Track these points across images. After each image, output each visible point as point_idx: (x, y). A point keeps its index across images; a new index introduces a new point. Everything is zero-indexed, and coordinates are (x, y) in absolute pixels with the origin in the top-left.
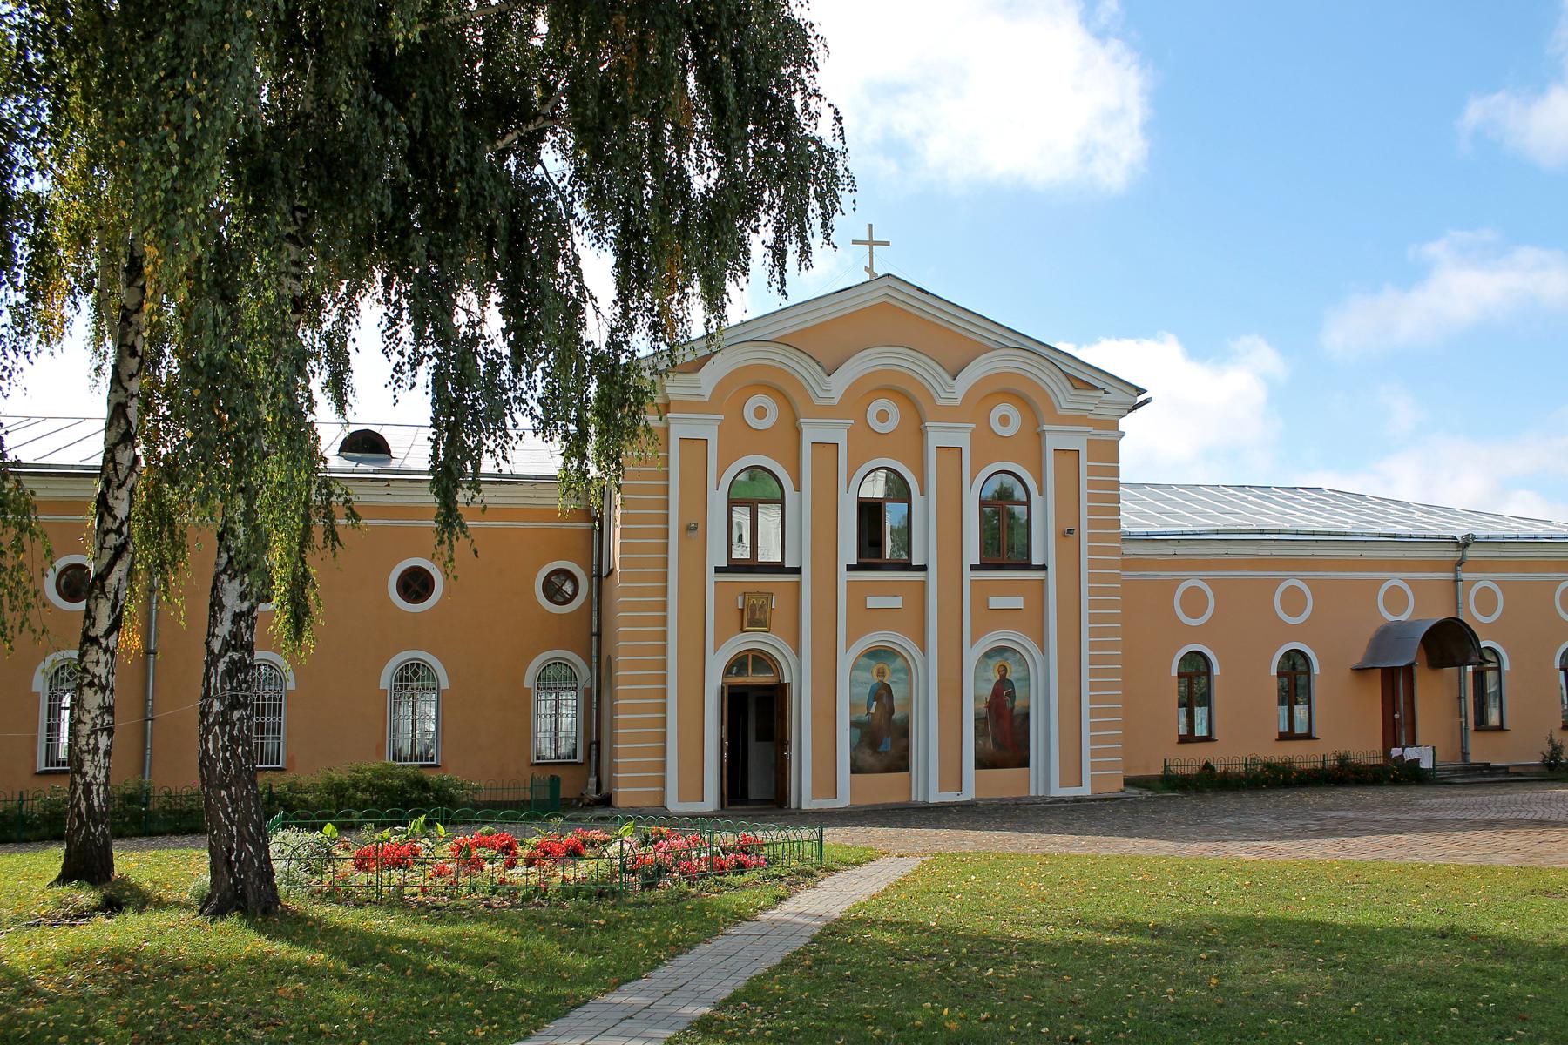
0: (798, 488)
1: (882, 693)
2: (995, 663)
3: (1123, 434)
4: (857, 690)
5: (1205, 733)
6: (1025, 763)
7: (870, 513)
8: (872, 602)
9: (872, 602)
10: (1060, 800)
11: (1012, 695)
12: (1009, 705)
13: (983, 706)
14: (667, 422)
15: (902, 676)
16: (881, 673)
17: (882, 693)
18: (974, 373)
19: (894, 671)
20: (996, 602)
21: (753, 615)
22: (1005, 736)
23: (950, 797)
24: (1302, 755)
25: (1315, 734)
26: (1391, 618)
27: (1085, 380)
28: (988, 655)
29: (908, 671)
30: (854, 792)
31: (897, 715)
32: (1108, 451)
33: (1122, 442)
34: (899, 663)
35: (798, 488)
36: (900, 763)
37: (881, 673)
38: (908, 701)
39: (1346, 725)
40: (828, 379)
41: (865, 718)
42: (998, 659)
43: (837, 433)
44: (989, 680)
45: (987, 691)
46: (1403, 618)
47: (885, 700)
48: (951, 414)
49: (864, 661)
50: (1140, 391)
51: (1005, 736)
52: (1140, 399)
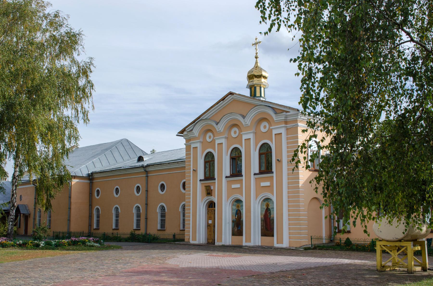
2: (265, 203)
4: (233, 211)
12: (269, 217)
13: (263, 216)
16: (238, 207)
20: (263, 184)
22: (268, 228)
23: (248, 244)
37: (238, 207)
42: (266, 202)
44: (264, 208)
45: (264, 213)
47: (239, 215)
49: (235, 203)
51: (268, 228)
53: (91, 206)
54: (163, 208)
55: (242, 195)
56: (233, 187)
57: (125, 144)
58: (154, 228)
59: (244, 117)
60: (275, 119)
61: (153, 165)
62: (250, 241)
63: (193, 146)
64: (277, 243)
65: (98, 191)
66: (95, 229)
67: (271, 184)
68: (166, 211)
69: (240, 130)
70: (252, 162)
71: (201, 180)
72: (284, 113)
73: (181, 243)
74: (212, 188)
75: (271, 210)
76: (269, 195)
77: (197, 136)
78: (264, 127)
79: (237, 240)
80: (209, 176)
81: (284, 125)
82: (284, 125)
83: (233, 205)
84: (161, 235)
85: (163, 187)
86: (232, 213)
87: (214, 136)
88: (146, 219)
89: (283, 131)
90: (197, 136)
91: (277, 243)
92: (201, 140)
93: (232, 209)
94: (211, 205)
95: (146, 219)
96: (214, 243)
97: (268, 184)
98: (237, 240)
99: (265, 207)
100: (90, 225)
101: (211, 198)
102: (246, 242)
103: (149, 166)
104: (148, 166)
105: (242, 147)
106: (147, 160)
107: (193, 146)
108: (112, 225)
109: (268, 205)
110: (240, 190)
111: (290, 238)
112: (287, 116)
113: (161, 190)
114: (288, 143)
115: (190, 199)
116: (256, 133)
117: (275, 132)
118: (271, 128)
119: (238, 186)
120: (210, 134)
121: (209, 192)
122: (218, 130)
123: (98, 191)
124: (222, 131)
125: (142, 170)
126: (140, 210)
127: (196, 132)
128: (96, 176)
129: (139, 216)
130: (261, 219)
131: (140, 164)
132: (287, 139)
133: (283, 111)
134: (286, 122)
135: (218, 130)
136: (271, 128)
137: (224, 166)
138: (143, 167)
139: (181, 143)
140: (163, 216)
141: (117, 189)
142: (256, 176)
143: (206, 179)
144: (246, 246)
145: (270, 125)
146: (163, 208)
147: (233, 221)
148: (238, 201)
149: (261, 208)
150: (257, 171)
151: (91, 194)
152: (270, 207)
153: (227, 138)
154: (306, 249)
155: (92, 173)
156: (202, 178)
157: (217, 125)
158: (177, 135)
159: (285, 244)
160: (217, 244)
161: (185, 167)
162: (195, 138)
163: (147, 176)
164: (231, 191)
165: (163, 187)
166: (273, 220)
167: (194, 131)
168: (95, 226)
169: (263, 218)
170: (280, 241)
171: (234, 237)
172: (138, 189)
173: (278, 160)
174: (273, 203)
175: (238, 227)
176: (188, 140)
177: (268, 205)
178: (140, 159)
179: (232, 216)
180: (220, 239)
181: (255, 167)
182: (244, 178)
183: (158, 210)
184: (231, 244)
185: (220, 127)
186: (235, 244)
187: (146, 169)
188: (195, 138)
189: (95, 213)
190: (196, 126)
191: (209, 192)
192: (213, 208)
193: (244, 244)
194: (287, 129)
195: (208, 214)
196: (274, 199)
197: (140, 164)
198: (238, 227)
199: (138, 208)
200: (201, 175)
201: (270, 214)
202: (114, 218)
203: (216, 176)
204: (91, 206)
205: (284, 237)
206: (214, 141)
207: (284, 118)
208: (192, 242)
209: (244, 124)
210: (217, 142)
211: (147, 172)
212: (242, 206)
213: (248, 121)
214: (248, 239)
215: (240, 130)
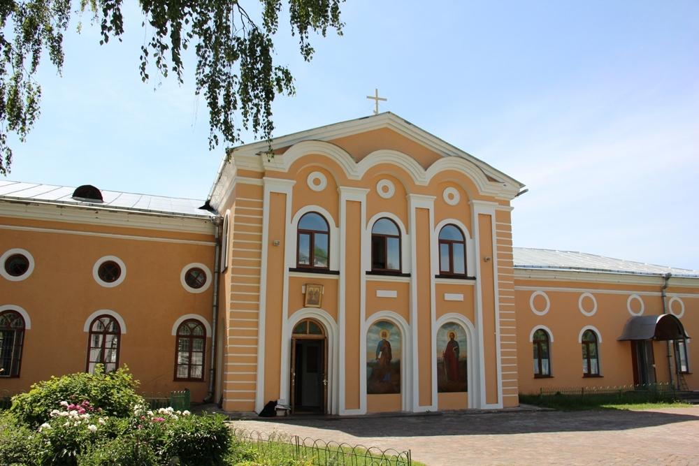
0: (338, 225)
1: (385, 348)
3: (512, 208)
4: (370, 345)
5: (547, 373)
6: (466, 390)
7: (379, 244)
8: (380, 293)
9: (380, 293)
10: (489, 412)
11: (457, 350)
12: (456, 355)
13: (441, 356)
14: (263, 183)
15: (396, 337)
16: (384, 335)
17: (385, 348)
18: (436, 168)
19: (392, 334)
21: (309, 299)
23: (424, 409)
24: (593, 386)
25: (690, 372)
26: (634, 315)
27: (493, 177)
29: (399, 334)
30: (369, 406)
31: (393, 360)
32: (505, 217)
33: (512, 212)
34: (394, 330)
35: (338, 225)
36: (395, 388)
38: (400, 351)
39: (615, 369)
40: (357, 165)
42: (449, 329)
43: (360, 195)
44: (444, 341)
45: (444, 347)
46: (640, 314)
47: (386, 350)
48: (422, 190)
50: (522, 185)
52: (521, 190)
56: (378, 296)
61: (27, 204)
80: (313, 263)
99: (448, 339)
109: (452, 336)
171: (372, 396)
175: (385, 375)
177: (452, 336)
185: (358, 170)
186: (375, 411)
201: (458, 352)
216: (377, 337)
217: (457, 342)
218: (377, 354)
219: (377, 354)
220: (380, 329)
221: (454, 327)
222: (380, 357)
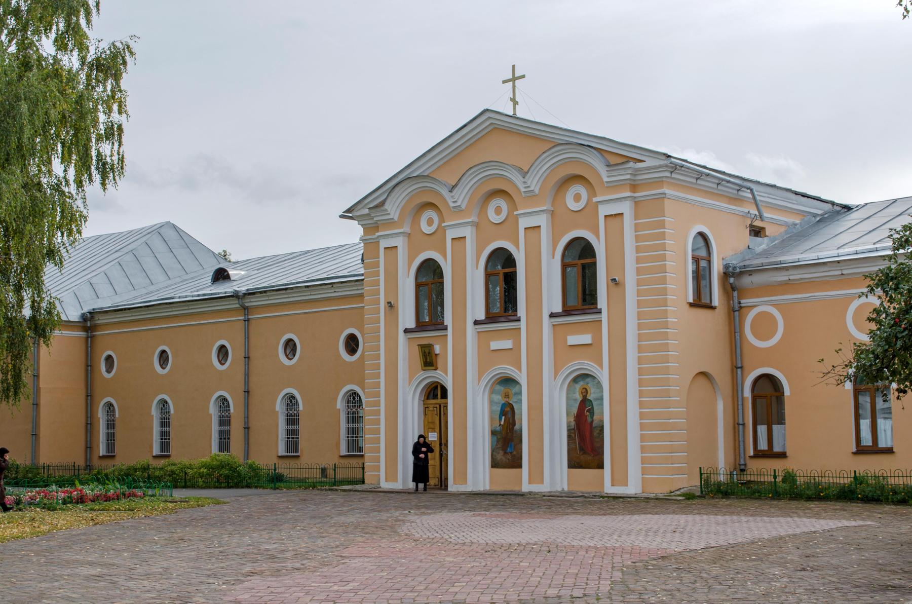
2: (578, 387)
11: (591, 411)
12: (589, 419)
13: (572, 420)
16: (507, 396)
20: (572, 340)
22: (586, 445)
23: (536, 488)
28: (575, 380)
31: (517, 427)
34: (517, 387)
41: (498, 428)
42: (581, 383)
44: (576, 400)
45: (575, 410)
47: (510, 415)
49: (498, 387)
51: (586, 445)
53: (90, 397)
54: (291, 400)
55: (520, 369)
57: (170, 234)
58: (268, 452)
59: (524, 174)
60: (606, 179)
62: (541, 481)
63: (384, 244)
64: (613, 485)
65: (109, 359)
66: (104, 457)
67: (593, 338)
68: (301, 408)
69: (513, 205)
70: (544, 283)
71: (406, 331)
72: (631, 164)
73: (359, 487)
74: (437, 349)
75: (595, 403)
76: (589, 366)
77: (396, 219)
78: (575, 199)
79: (505, 479)
80: (430, 318)
81: (628, 194)
82: (628, 194)
83: (492, 392)
84: (285, 469)
85: (290, 347)
86: (492, 412)
87: (442, 219)
88: (247, 428)
89: (626, 208)
90: (396, 219)
91: (613, 485)
92: (406, 229)
93: (491, 402)
94: (435, 393)
95: (247, 428)
96: (446, 486)
97: (586, 339)
98: (505, 479)
99: (579, 398)
100: (89, 447)
101: (437, 375)
102: (530, 483)
103: (254, 294)
104: (250, 294)
105: (518, 247)
106: (241, 280)
107: (384, 244)
108: (151, 447)
109: (585, 392)
110: (512, 354)
111: (644, 471)
112: (637, 170)
113: (287, 356)
114: (638, 238)
115: (378, 376)
116: (552, 213)
117: (604, 210)
118: (595, 200)
119: (507, 344)
120: (432, 214)
121: (428, 359)
122: (452, 205)
123: (109, 359)
124: (463, 207)
125: (234, 304)
126: (228, 406)
127: (393, 209)
128: (101, 320)
129: (225, 421)
130: (568, 426)
131: (223, 289)
132: (637, 228)
133: (629, 159)
134: (634, 187)
135: (452, 205)
136: (595, 200)
137: (469, 293)
138: (236, 296)
139: (354, 232)
140: (292, 420)
141: (164, 352)
142: (556, 320)
143: (421, 326)
144: (530, 493)
145: (592, 192)
146: (291, 400)
147: (493, 433)
148: (508, 381)
149: (568, 399)
150: (558, 309)
151: (89, 367)
152: (591, 397)
153: (476, 225)
154: (689, 496)
155: (93, 313)
156: (412, 324)
157: (451, 191)
158: (341, 216)
159: (633, 488)
160: (452, 487)
161: (361, 296)
162: (390, 223)
163: (247, 320)
164: (487, 357)
165: (290, 347)
166: (602, 427)
167: (387, 206)
168: (102, 451)
169: (573, 423)
170: (620, 478)
172: (223, 352)
173: (614, 280)
174: (599, 385)
175: (507, 446)
176: (368, 229)
177: (585, 392)
178: (221, 275)
179: (492, 419)
180: (462, 476)
181: (552, 298)
182: (523, 324)
183: (279, 406)
184: (488, 488)
187: (243, 301)
188: (390, 223)
189: (101, 415)
190: (393, 194)
191: (428, 359)
192: (439, 401)
193: (526, 488)
194: (637, 203)
195: (425, 414)
196: (604, 377)
197: (223, 289)
198: (507, 446)
199: (223, 401)
200: (407, 318)
201: (592, 414)
202: (156, 429)
203: (448, 320)
204: (90, 397)
205: (630, 467)
206: (441, 231)
207: (628, 177)
208: (385, 485)
209: (523, 190)
210: (450, 234)
211: (246, 309)
212: (520, 393)
213: (534, 183)
214: (537, 475)
215: (513, 205)
216: (499, 399)
217: (591, 401)
218: (500, 420)
219: (500, 420)
220: (502, 388)
221: (588, 380)
222: (502, 423)
